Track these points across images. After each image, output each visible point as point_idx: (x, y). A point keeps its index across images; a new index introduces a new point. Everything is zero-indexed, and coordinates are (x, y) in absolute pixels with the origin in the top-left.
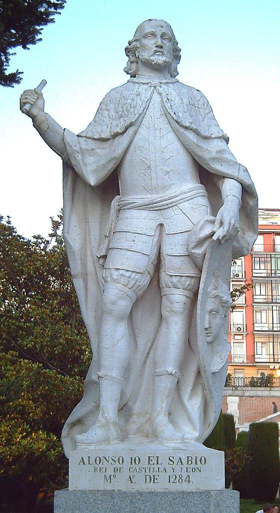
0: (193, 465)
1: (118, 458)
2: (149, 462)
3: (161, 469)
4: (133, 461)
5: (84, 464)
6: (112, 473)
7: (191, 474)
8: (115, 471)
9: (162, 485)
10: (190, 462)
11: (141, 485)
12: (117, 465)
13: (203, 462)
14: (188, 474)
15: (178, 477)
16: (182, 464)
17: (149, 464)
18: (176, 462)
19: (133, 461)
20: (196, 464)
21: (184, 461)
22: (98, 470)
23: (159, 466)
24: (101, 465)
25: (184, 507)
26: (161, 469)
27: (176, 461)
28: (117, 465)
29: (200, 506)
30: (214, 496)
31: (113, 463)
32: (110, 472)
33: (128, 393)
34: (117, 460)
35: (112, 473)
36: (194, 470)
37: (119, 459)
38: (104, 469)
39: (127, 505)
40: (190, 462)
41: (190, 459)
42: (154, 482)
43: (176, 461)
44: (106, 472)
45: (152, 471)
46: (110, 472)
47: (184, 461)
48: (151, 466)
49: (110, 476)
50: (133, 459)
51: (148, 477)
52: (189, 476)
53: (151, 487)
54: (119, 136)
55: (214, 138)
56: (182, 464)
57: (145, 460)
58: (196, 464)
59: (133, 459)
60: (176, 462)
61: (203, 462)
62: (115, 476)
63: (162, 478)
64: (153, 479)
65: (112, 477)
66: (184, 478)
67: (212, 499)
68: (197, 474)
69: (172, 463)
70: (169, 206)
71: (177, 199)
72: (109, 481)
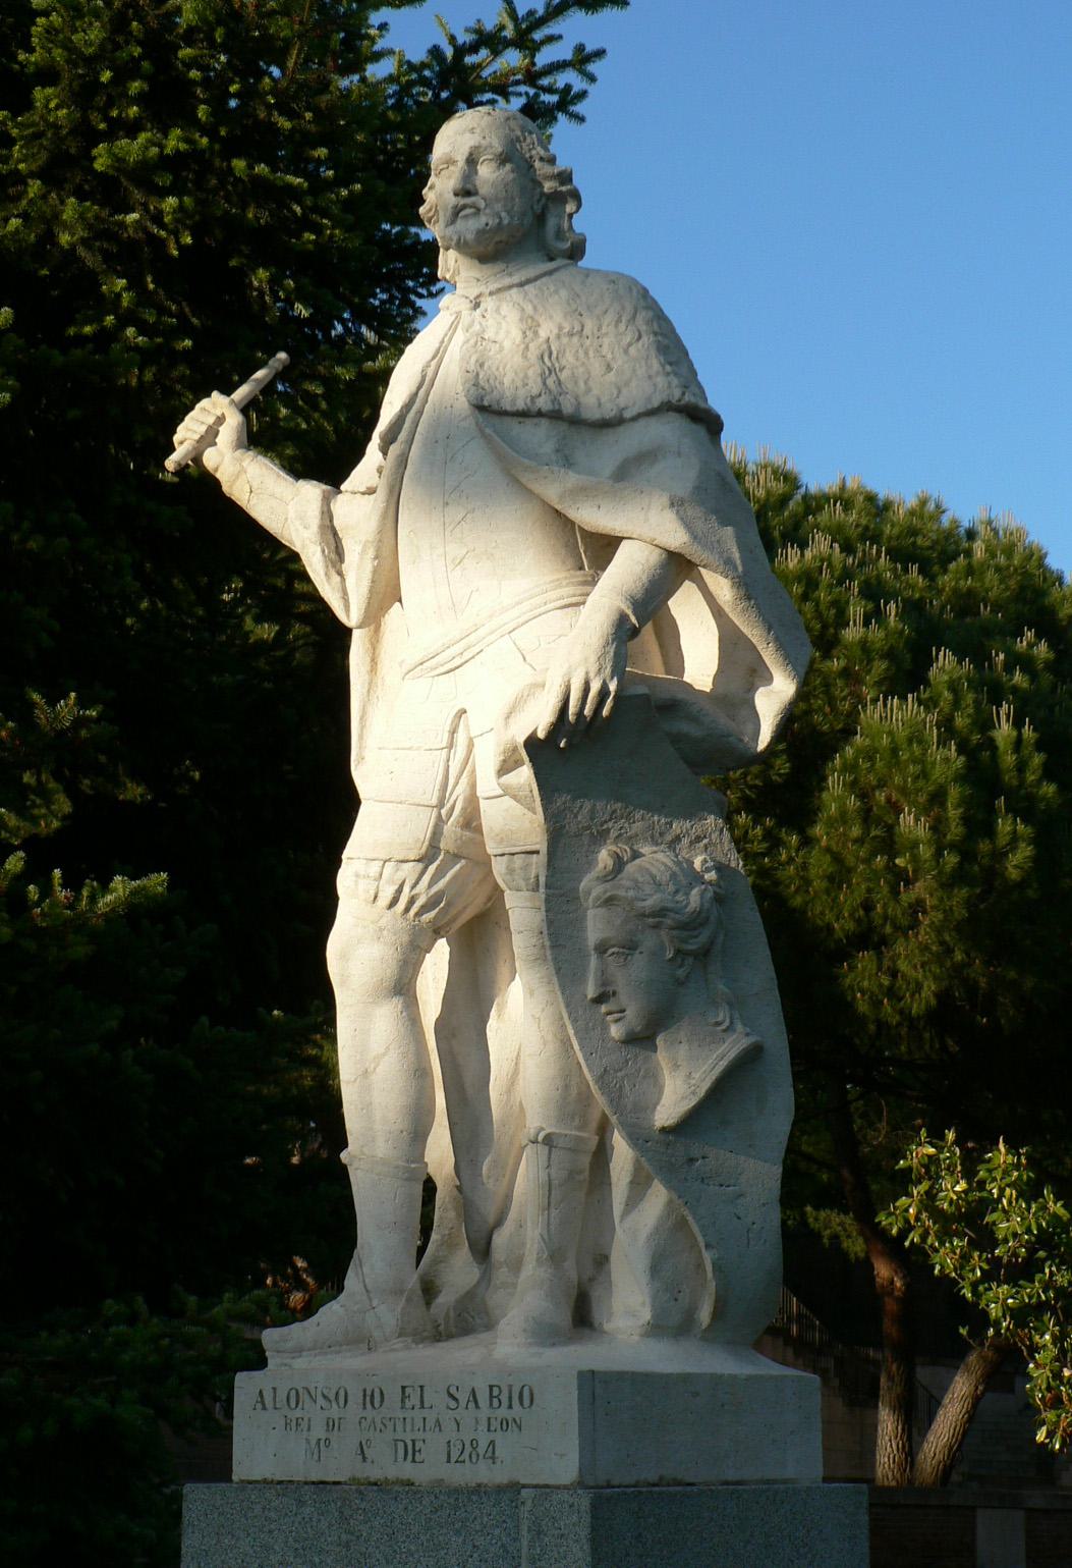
0: (503, 1412)
1: (334, 1392)
2: (403, 1401)
3: (430, 1423)
4: (368, 1398)
5: (264, 1408)
8: (328, 1430)
9: (431, 1469)
10: (495, 1402)
11: (386, 1466)
12: (335, 1412)
13: (526, 1402)
14: (492, 1436)
16: (477, 1406)
18: (463, 1403)
19: (368, 1398)
20: (510, 1407)
21: (483, 1398)
23: (426, 1413)
24: (298, 1413)
25: (458, 1533)
26: (430, 1423)
27: (463, 1397)
28: (335, 1412)
29: (497, 1532)
30: (529, 1503)
32: (319, 1432)
34: (332, 1398)
36: (505, 1424)
38: (306, 1419)
39: (330, 1525)
40: (495, 1402)
41: (496, 1392)
42: (414, 1461)
43: (463, 1397)
44: (309, 1429)
45: (408, 1428)
46: (319, 1432)
47: (483, 1398)
48: (409, 1414)
50: (369, 1393)
51: (401, 1445)
52: (492, 1443)
53: (407, 1471)
54: (640, 420)
55: (634, 419)
56: (477, 1406)
57: (393, 1395)
58: (510, 1407)
59: (369, 1393)
60: (463, 1403)
61: (526, 1402)
63: (433, 1448)
64: (412, 1452)
65: (322, 1442)
66: (481, 1450)
69: (453, 1404)
70: (467, 656)
71: (482, 632)
72: (316, 1457)
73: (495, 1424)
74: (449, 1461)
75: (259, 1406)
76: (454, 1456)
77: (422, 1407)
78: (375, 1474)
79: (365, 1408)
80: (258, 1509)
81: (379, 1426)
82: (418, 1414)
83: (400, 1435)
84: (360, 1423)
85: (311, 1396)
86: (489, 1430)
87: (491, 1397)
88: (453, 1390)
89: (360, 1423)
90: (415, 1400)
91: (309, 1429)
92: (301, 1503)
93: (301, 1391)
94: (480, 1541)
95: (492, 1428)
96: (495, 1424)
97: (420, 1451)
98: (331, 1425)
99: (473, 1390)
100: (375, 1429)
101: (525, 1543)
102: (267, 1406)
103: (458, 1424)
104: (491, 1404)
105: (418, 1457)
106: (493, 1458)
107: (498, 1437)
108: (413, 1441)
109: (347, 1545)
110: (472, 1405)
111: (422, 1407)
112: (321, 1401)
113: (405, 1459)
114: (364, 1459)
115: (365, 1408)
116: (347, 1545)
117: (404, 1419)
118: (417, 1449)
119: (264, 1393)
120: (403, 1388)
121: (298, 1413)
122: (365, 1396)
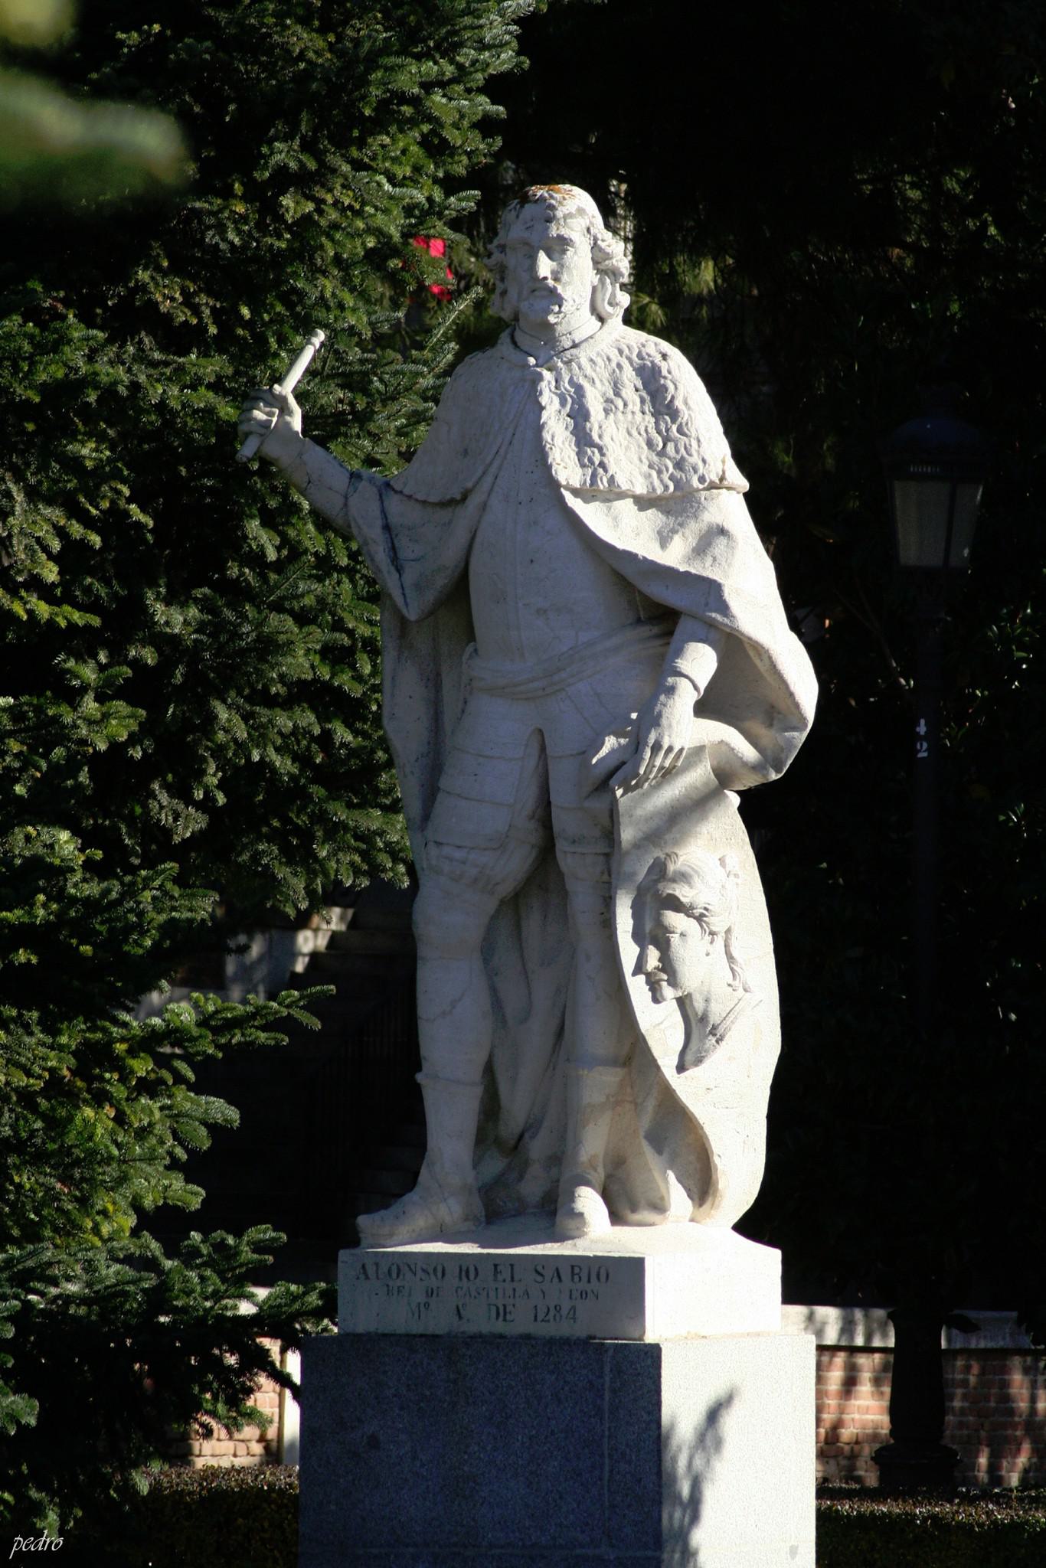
0: (583, 1285)
4: (464, 1273)
5: (367, 1278)
6: (422, 1299)
9: (521, 1323)
10: (576, 1278)
12: (434, 1282)
13: (603, 1277)
15: (552, 1312)
18: (548, 1278)
19: (464, 1273)
20: (589, 1281)
21: (566, 1275)
23: (515, 1285)
24: (399, 1283)
27: (549, 1273)
28: (434, 1282)
29: (584, 1372)
34: (431, 1271)
35: (422, 1299)
36: (584, 1295)
37: (435, 1270)
40: (576, 1278)
41: (577, 1270)
42: (505, 1320)
43: (549, 1273)
44: (410, 1295)
45: (500, 1295)
46: (419, 1297)
47: (566, 1275)
49: (419, 1304)
50: (464, 1268)
52: (573, 1308)
53: (500, 1327)
58: (589, 1281)
59: (464, 1268)
62: (427, 1305)
64: (502, 1313)
65: (422, 1306)
66: (564, 1312)
69: (539, 1279)
73: (576, 1294)
75: (362, 1277)
76: (540, 1316)
78: (471, 1328)
79: (460, 1279)
81: (474, 1293)
84: (457, 1292)
85: (411, 1269)
86: (571, 1298)
88: (539, 1268)
89: (457, 1292)
90: (507, 1274)
91: (410, 1295)
93: (401, 1265)
95: (574, 1297)
96: (576, 1294)
97: (510, 1313)
98: (430, 1293)
99: (557, 1269)
100: (470, 1296)
101: (607, 1379)
102: (370, 1276)
103: (544, 1293)
104: (573, 1280)
105: (508, 1317)
106: (574, 1319)
108: (505, 1306)
110: (556, 1280)
112: (420, 1274)
113: (497, 1317)
115: (460, 1279)
117: (497, 1289)
118: (508, 1310)
120: (496, 1266)
121: (399, 1283)
122: (461, 1270)
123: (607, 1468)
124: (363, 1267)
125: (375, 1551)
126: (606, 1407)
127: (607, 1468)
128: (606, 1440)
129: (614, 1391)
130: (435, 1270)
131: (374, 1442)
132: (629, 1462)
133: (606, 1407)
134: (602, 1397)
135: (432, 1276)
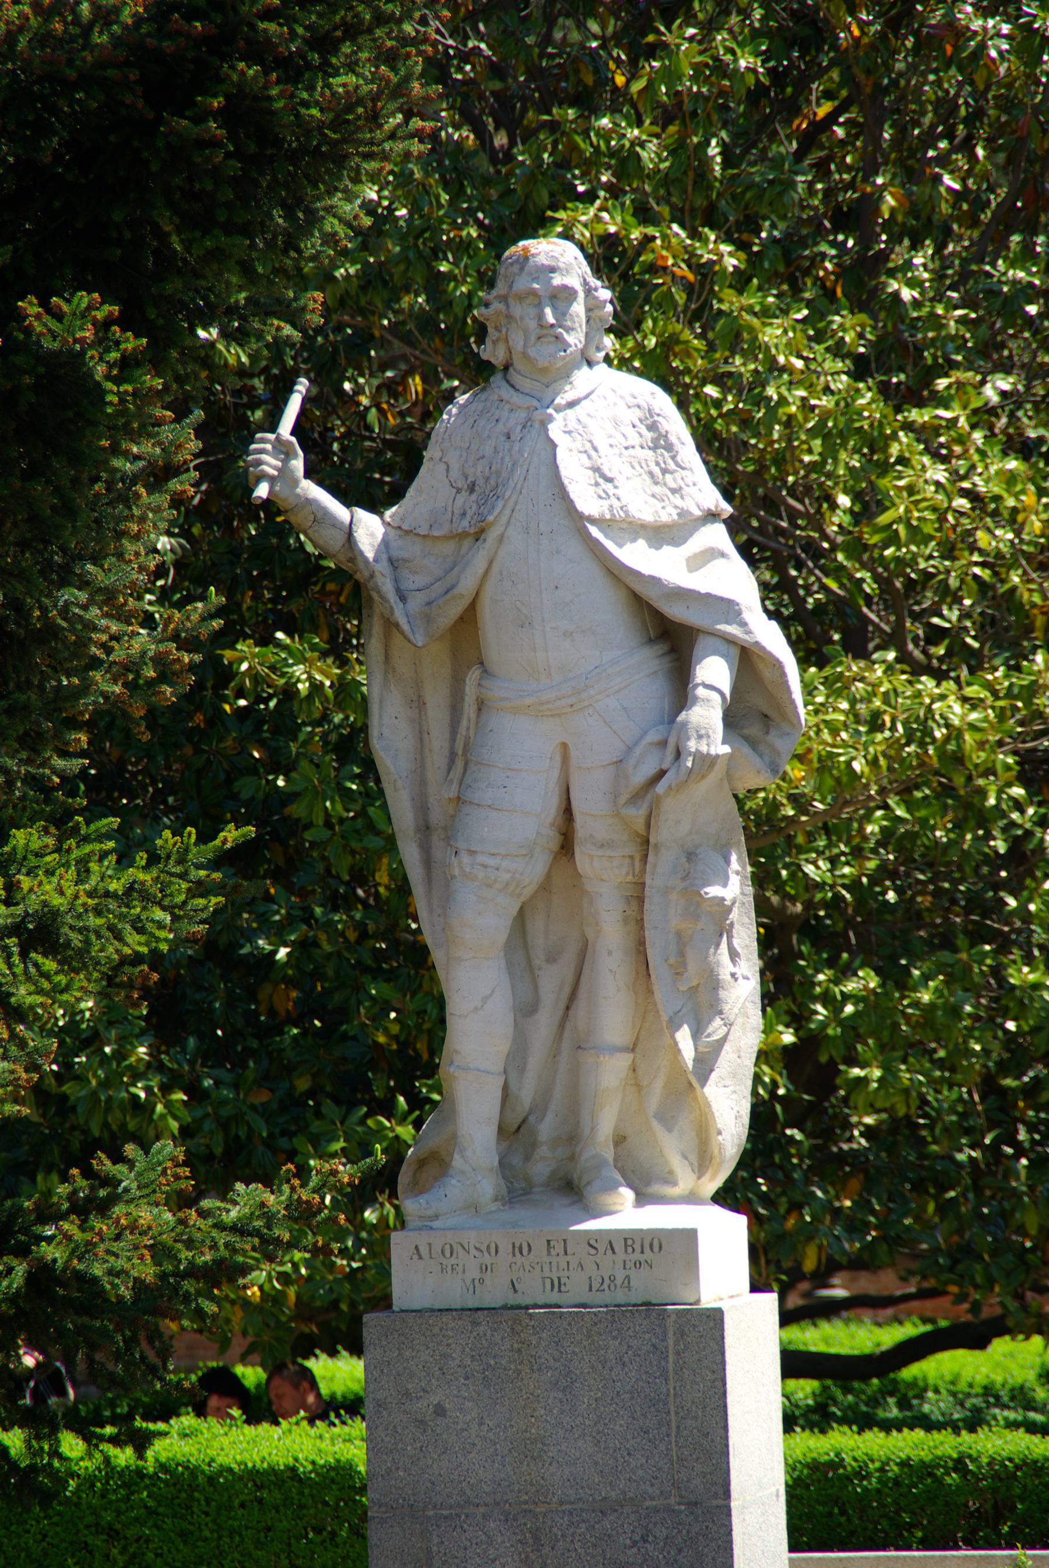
0: (637, 1256)
5: (420, 1258)
6: (477, 1275)
7: (633, 1273)
10: (630, 1250)
13: (656, 1248)
14: (628, 1272)
15: (607, 1281)
16: (614, 1252)
17: (549, 1254)
18: (601, 1251)
21: (619, 1247)
22: (449, 1269)
23: (569, 1258)
24: (453, 1261)
25: (615, 1338)
27: (602, 1246)
28: (487, 1259)
29: (647, 1336)
30: (674, 1317)
31: (477, 1254)
32: (474, 1273)
33: (526, 1094)
34: (484, 1249)
35: (477, 1275)
36: (638, 1265)
37: (488, 1247)
39: (503, 1338)
40: (630, 1250)
41: (630, 1242)
42: (560, 1291)
43: (602, 1246)
45: (554, 1268)
46: (474, 1273)
47: (619, 1247)
48: (554, 1260)
50: (517, 1245)
52: (628, 1277)
53: (554, 1297)
56: (614, 1252)
59: (517, 1245)
60: (601, 1251)
62: (482, 1281)
64: (558, 1285)
66: (619, 1282)
67: (670, 1322)
68: (644, 1271)
69: (593, 1251)
72: (471, 1291)
74: (591, 1290)
75: (416, 1257)
77: (566, 1253)
80: (436, 1330)
81: (528, 1268)
82: (563, 1260)
83: (547, 1272)
87: (626, 1246)
88: (592, 1242)
92: (475, 1324)
93: (455, 1246)
94: (634, 1343)
98: (484, 1269)
99: (611, 1243)
105: (563, 1288)
106: (629, 1288)
107: (633, 1273)
109: (519, 1351)
110: (609, 1252)
111: (566, 1253)
112: (473, 1251)
114: (515, 1291)
116: (519, 1351)
119: (421, 1248)
120: (548, 1241)
121: (453, 1261)
123: (674, 1425)
124: (417, 1247)
125: (445, 1512)
126: (671, 1366)
127: (674, 1425)
128: (671, 1398)
129: (678, 1353)
130: (488, 1247)
131: (440, 1411)
132: (696, 1418)
133: (671, 1366)
134: (666, 1358)
135: (486, 1254)
